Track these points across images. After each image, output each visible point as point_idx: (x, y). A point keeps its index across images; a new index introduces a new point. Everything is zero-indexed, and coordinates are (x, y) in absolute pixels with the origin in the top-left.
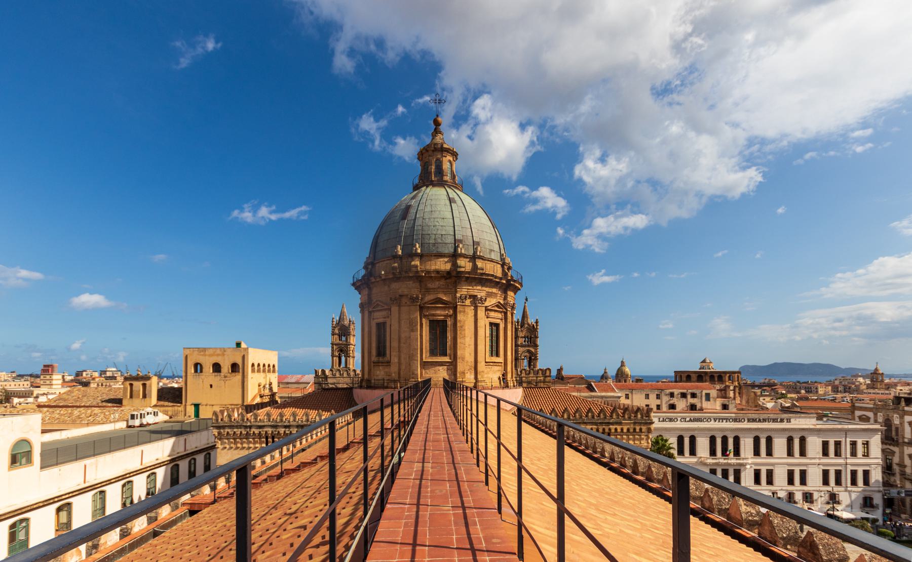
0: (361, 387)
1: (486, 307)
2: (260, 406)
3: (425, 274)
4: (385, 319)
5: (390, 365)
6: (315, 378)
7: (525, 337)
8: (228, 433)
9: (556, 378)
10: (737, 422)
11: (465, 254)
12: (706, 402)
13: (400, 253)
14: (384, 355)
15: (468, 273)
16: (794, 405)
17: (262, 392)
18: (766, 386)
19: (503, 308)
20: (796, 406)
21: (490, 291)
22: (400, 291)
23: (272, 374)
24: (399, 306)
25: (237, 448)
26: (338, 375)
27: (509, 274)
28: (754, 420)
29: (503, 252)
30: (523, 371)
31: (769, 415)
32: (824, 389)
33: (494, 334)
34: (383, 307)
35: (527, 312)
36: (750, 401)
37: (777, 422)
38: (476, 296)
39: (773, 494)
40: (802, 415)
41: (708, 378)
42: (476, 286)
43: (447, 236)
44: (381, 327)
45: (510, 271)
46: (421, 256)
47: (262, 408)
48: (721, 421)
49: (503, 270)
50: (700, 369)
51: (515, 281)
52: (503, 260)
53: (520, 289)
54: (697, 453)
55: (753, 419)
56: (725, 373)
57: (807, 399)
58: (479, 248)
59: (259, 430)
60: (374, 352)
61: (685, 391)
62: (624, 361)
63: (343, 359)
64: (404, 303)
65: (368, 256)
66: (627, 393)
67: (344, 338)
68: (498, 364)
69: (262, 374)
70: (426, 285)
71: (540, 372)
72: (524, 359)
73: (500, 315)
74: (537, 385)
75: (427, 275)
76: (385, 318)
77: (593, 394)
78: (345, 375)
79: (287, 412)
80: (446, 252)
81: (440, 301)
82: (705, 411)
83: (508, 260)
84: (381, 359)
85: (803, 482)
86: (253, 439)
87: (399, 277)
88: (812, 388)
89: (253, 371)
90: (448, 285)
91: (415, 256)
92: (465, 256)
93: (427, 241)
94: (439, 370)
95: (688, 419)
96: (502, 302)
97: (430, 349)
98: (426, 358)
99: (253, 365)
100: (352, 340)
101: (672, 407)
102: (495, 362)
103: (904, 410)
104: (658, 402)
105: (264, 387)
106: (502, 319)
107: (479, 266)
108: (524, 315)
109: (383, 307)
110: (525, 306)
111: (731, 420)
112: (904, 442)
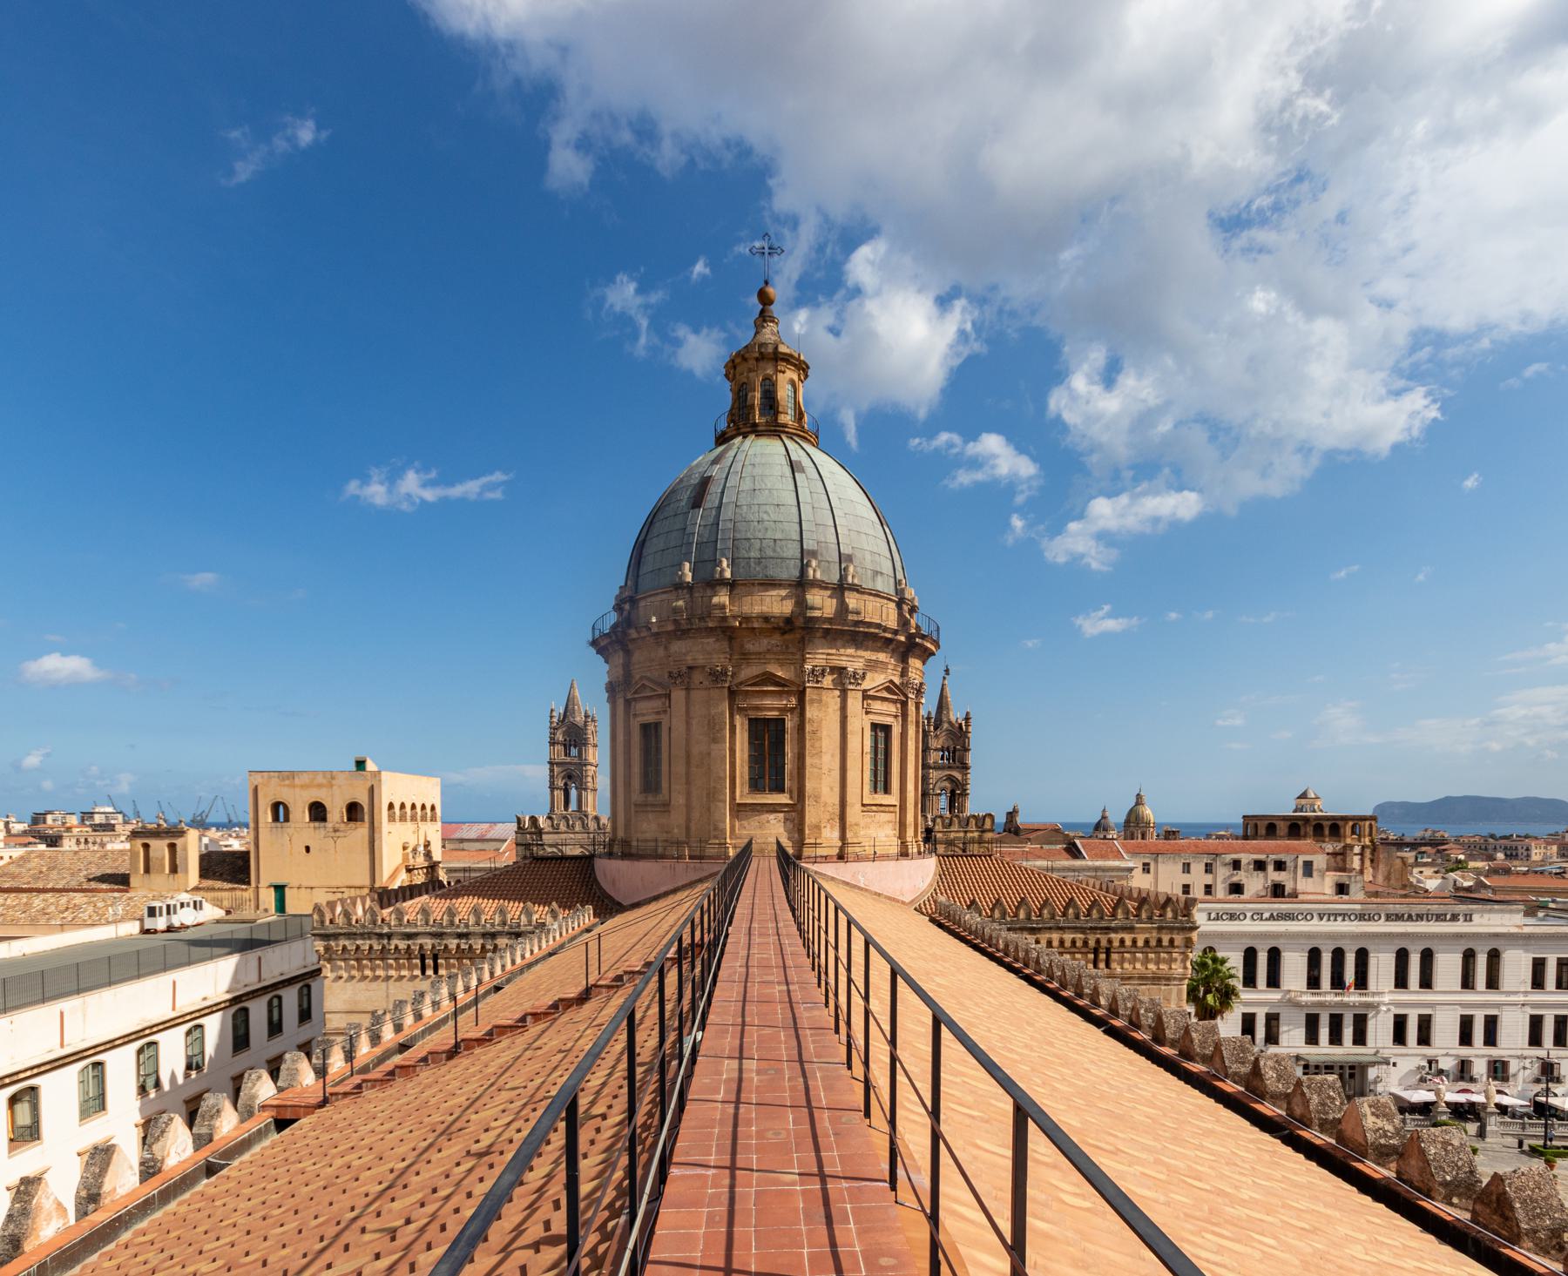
0: (610, 855)
1: (865, 691)
2: (408, 893)
3: (740, 623)
4: (658, 717)
6: (516, 833)
7: (942, 750)
8: (344, 948)
9: (1005, 831)
10: (1365, 920)
11: (823, 581)
12: (1304, 880)
13: (689, 578)
15: (829, 620)
16: (1480, 885)
17: (411, 862)
18: (1425, 845)
19: (899, 693)
20: (1485, 886)
21: (874, 658)
22: (689, 658)
23: (429, 823)
24: (688, 689)
25: (364, 978)
26: (563, 827)
27: (913, 622)
28: (1398, 917)
29: (900, 576)
30: (939, 820)
31: (1429, 907)
32: (1543, 851)
33: (881, 746)
34: (655, 690)
35: (947, 697)
36: (1393, 876)
37: (1445, 920)
38: (845, 668)
39: (1430, 1062)
40: (1496, 907)
41: (1310, 830)
42: (844, 647)
43: (783, 543)
44: (650, 732)
45: (915, 615)
46: (732, 585)
47: (412, 898)
48: (1332, 918)
49: (900, 614)
50: (1295, 811)
51: (923, 637)
52: (900, 592)
53: (933, 654)
54: (1282, 983)
55: (1397, 915)
56: (1345, 819)
57: (1507, 871)
58: (851, 569)
59: (407, 942)
60: (636, 783)
61: (1262, 857)
62: (1142, 793)
63: (573, 793)
64: (697, 682)
65: (623, 584)
66: (1147, 861)
67: (574, 752)
68: (887, 809)
69: (410, 825)
70: (742, 646)
71: (973, 822)
72: (940, 794)
73: (892, 709)
74: (964, 851)
75: (744, 626)
76: (658, 713)
77: (1078, 863)
78: (578, 828)
79: (462, 905)
80: (784, 576)
81: (770, 679)
82: (1301, 897)
83: (910, 593)
84: (651, 799)
85: (1490, 1040)
86: (396, 959)
87: (689, 630)
88: (1519, 847)
89: (392, 819)
90: (787, 647)
91: (720, 585)
92: (822, 585)
93: (743, 553)
94: (768, 822)
95: (1266, 915)
96: (897, 680)
97: (750, 779)
98: (741, 796)
99: (391, 806)
100: (592, 755)
101: (1236, 889)
102: (881, 805)
104: (1208, 879)
105: (415, 850)
106: (896, 717)
107: (851, 606)
108: (942, 704)
109: (655, 690)
110: (943, 685)
111: (1352, 918)
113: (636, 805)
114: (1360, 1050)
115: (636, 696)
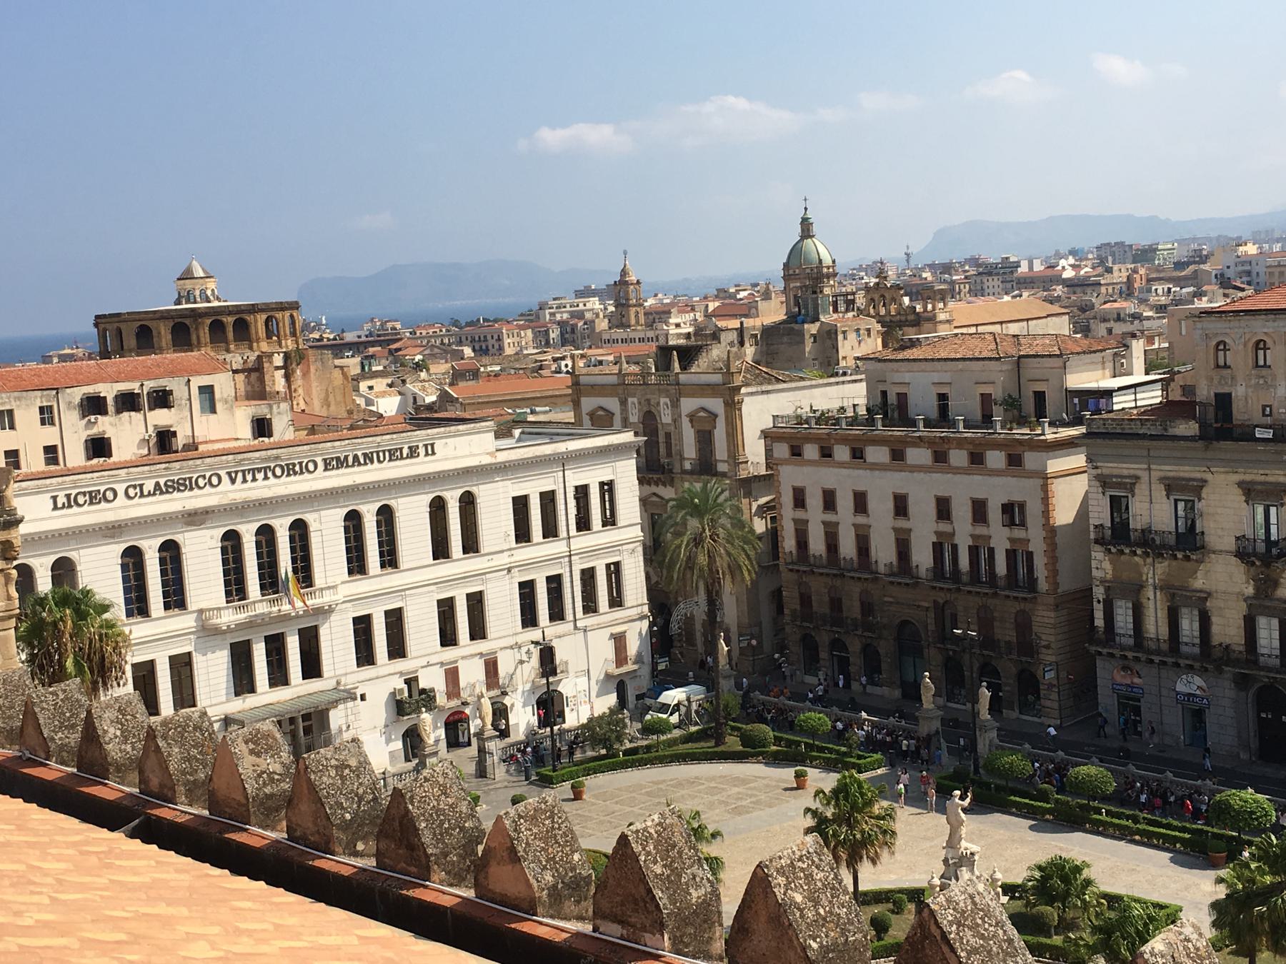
10: (295, 473)
12: (204, 418)
16: (445, 398)
18: (373, 344)
20: (453, 400)
28: (341, 463)
31: (378, 439)
32: (516, 339)
36: (331, 398)
37: (402, 458)
39: (407, 682)
40: (461, 427)
41: (205, 333)
48: (260, 476)
50: (178, 302)
54: (188, 600)
55: (338, 459)
56: (254, 309)
57: (475, 374)
61: (134, 386)
82: (202, 448)
85: (478, 631)
88: (489, 337)
95: (149, 486)
101: (99, 447)
103: (678, 384)
104: (49, 436)
111: (278, 471)
112: (684, 472)
114: (314, 685)
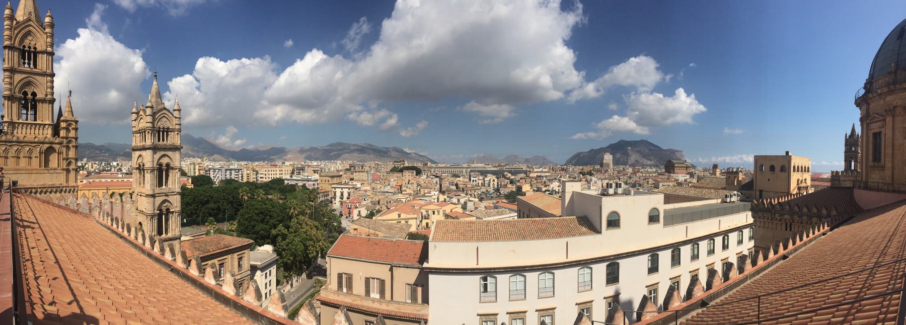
0: (859, 188)
5: (884, 170)
14: (879, 161)
23: (806, 173)
24: (894, 116)
44: (877, 136)
60: (871, 158)
76: (880, 128)
89: (794, 171)
99: (794, 167)
113: (870, 167)
115: (871, 121)
